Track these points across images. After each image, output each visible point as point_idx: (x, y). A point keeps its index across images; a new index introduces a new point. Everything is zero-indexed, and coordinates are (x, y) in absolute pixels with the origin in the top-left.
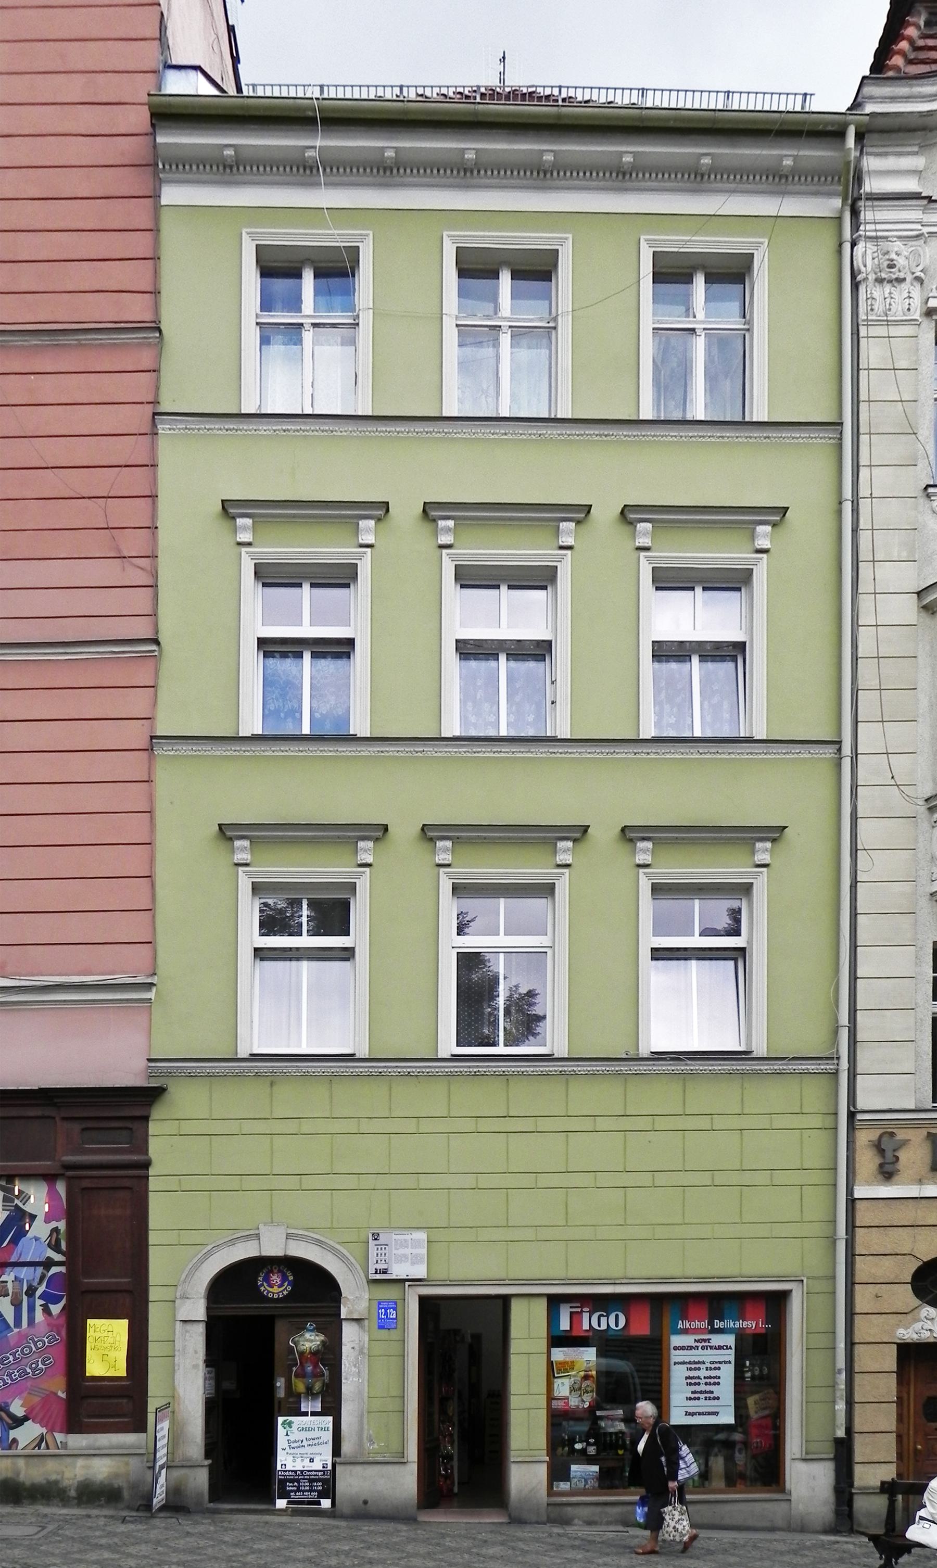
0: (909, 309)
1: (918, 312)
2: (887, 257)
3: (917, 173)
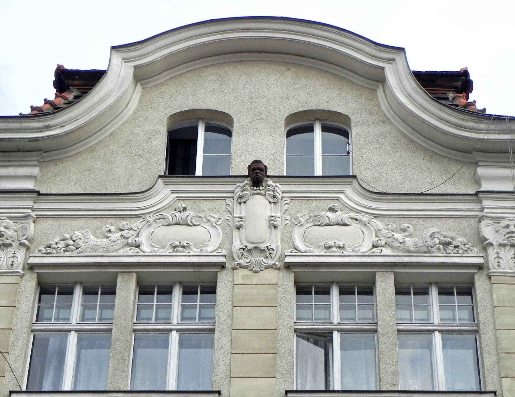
0: (12, 265)
1: (21, 267)
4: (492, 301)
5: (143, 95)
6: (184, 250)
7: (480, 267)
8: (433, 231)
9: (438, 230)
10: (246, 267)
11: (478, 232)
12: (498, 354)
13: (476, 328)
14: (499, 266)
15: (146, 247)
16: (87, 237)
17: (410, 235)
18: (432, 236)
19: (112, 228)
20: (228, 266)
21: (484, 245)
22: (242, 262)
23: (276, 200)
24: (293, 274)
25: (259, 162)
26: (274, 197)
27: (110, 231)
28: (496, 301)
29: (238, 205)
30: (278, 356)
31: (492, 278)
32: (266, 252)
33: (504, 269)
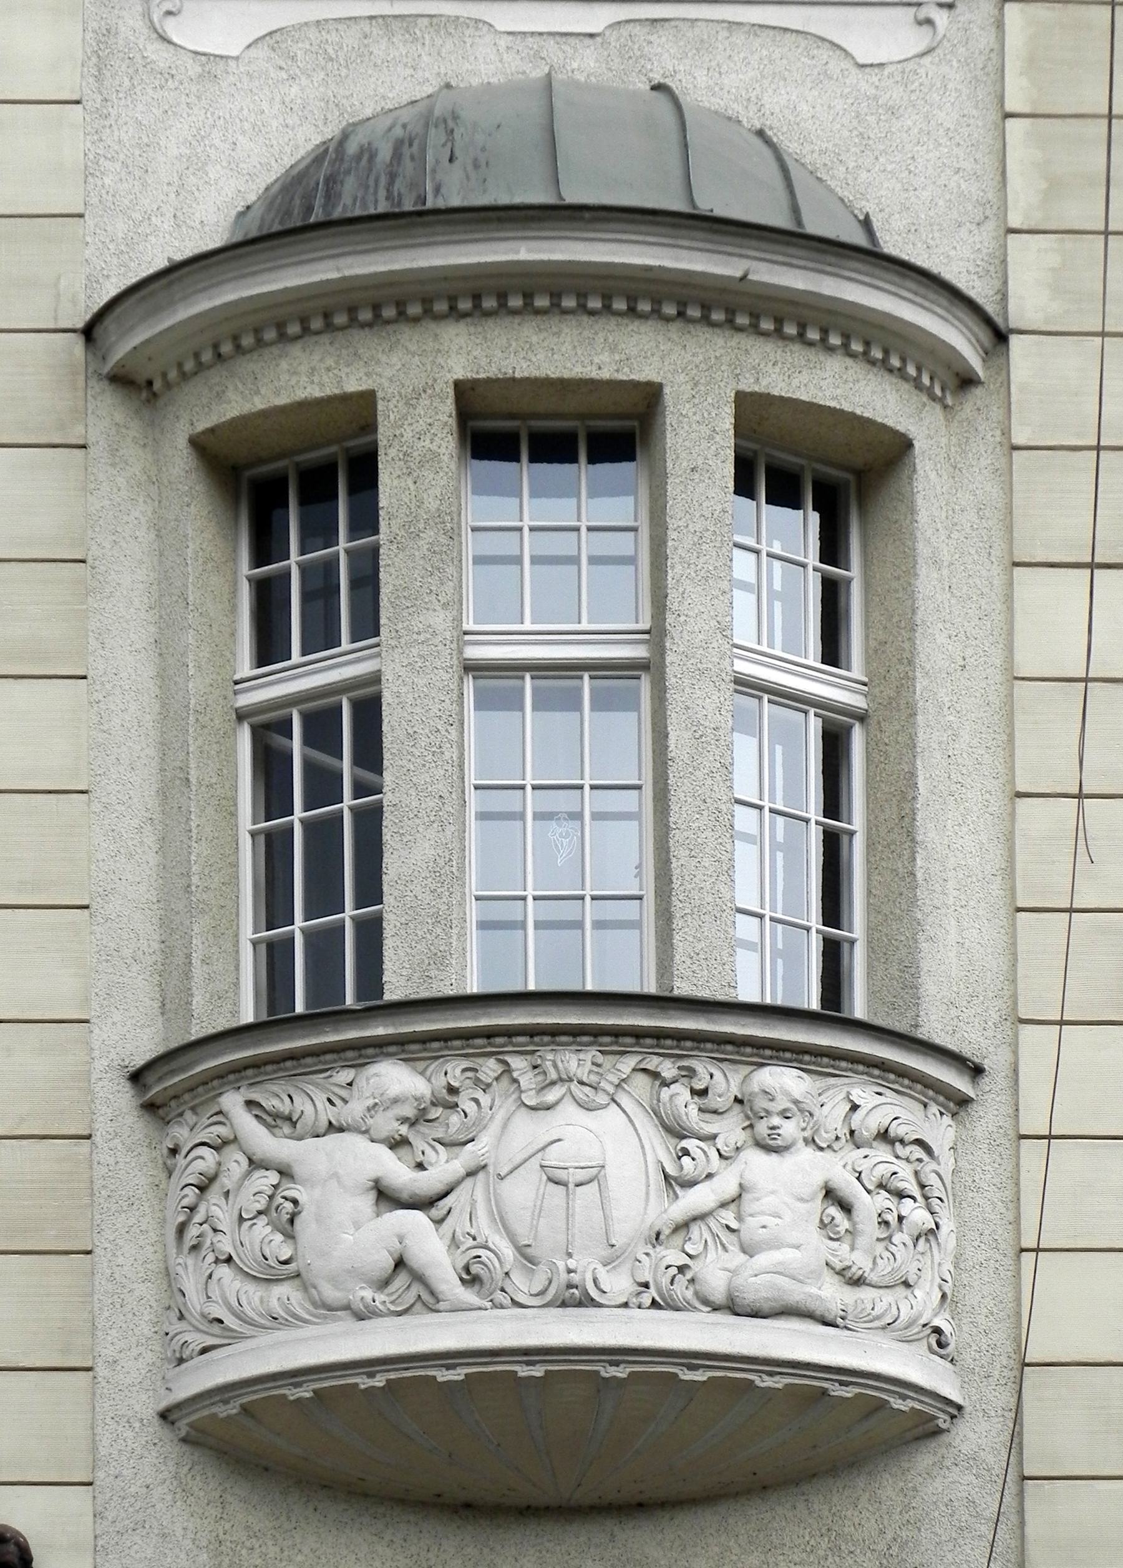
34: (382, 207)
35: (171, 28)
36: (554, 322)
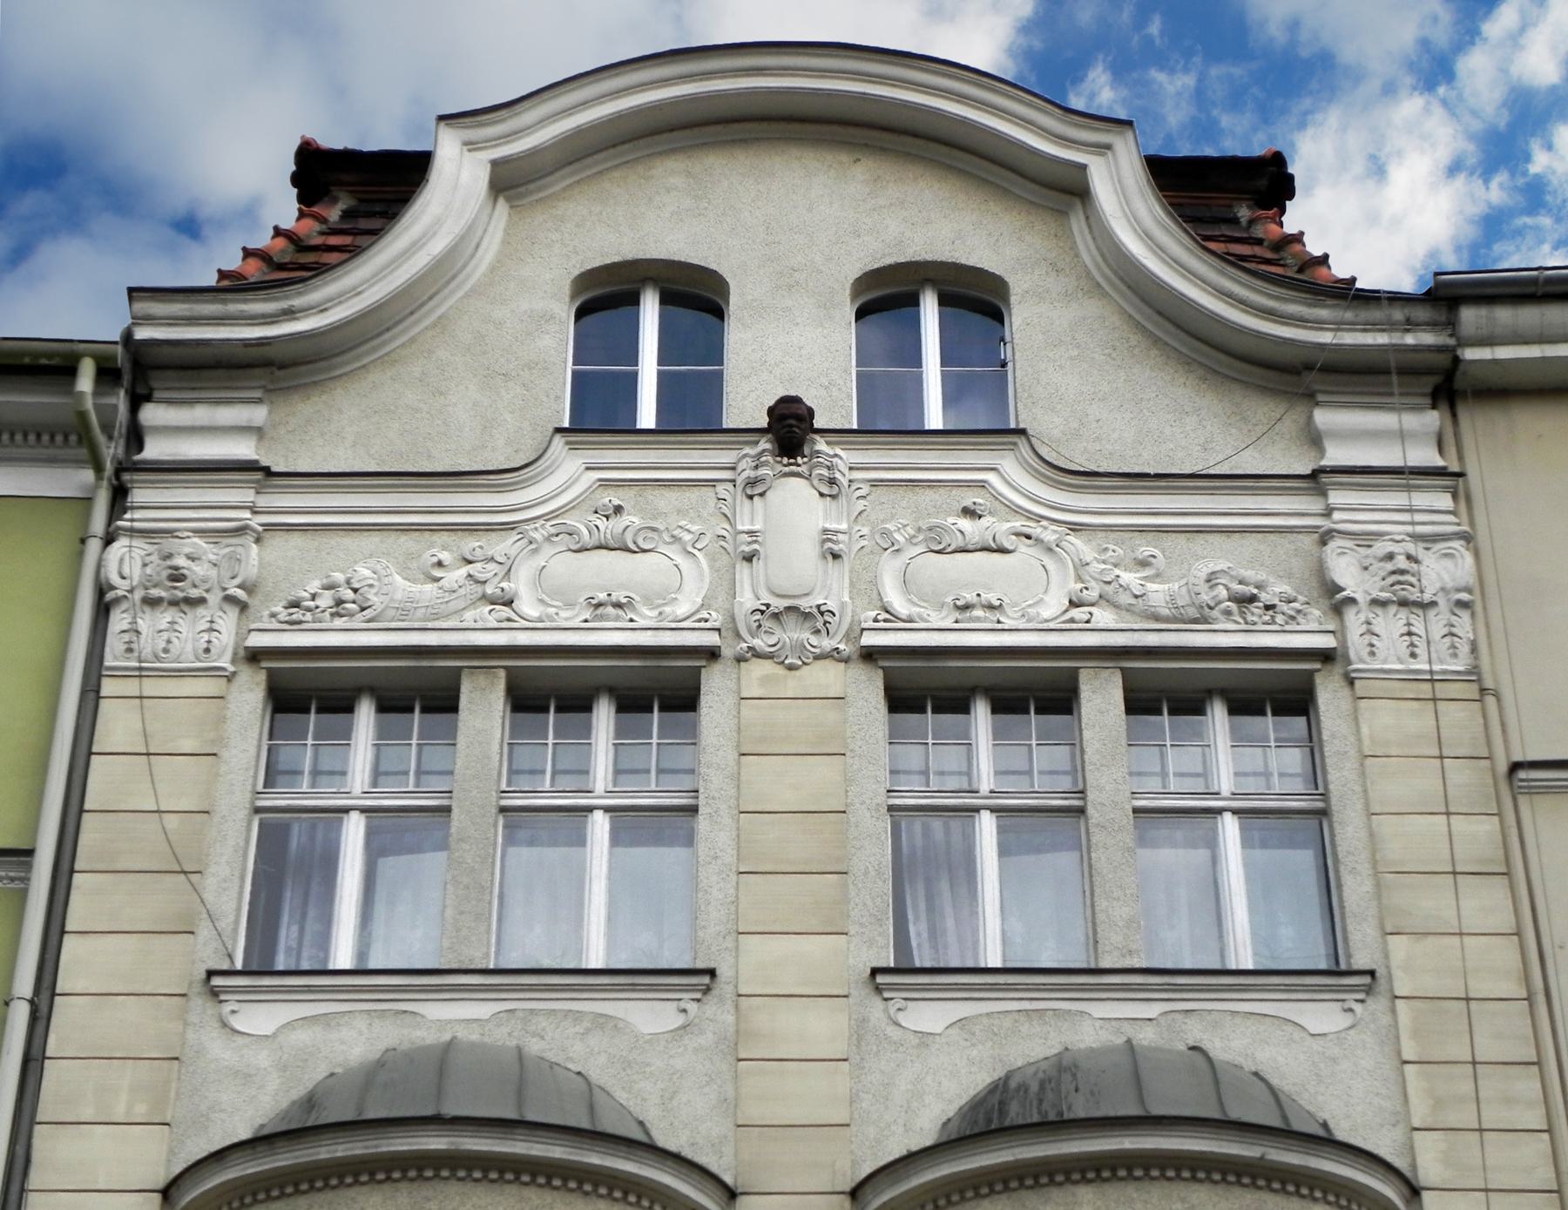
0: (207, 650)
1: (228, 655)
2: (169, 563)
3: (258, 432)
4: (1359, 740)
5: (511, 224)
6: (620, 612)
7: (1326, 656)
8: (1212, 567)
9: (1222, 565)
10: (769, 656)
11: (1321, 571)
12: (1376, 874)
13: (1320, 805)
14: (1372, 654)
15: (528, 606)
16: (386, 580)
17: (1157, 577)
18: (1211, 579)
19: (445, 556)
20: (727, 652)
21: (1336, 601)
22: (758, 643)
23: (835, 490)
24: (881, 672)
25: (796, 400)
26: (832, 482)
27: (440, 564)
28: (1366, 742)
29: (747, 502)
30: (850, 879)
31: (1358, 683)
32: (816, 618)
33: (1385, 662)
34: (1036, 1119)
35: (901, 1018)
36: (1146, 1184)
